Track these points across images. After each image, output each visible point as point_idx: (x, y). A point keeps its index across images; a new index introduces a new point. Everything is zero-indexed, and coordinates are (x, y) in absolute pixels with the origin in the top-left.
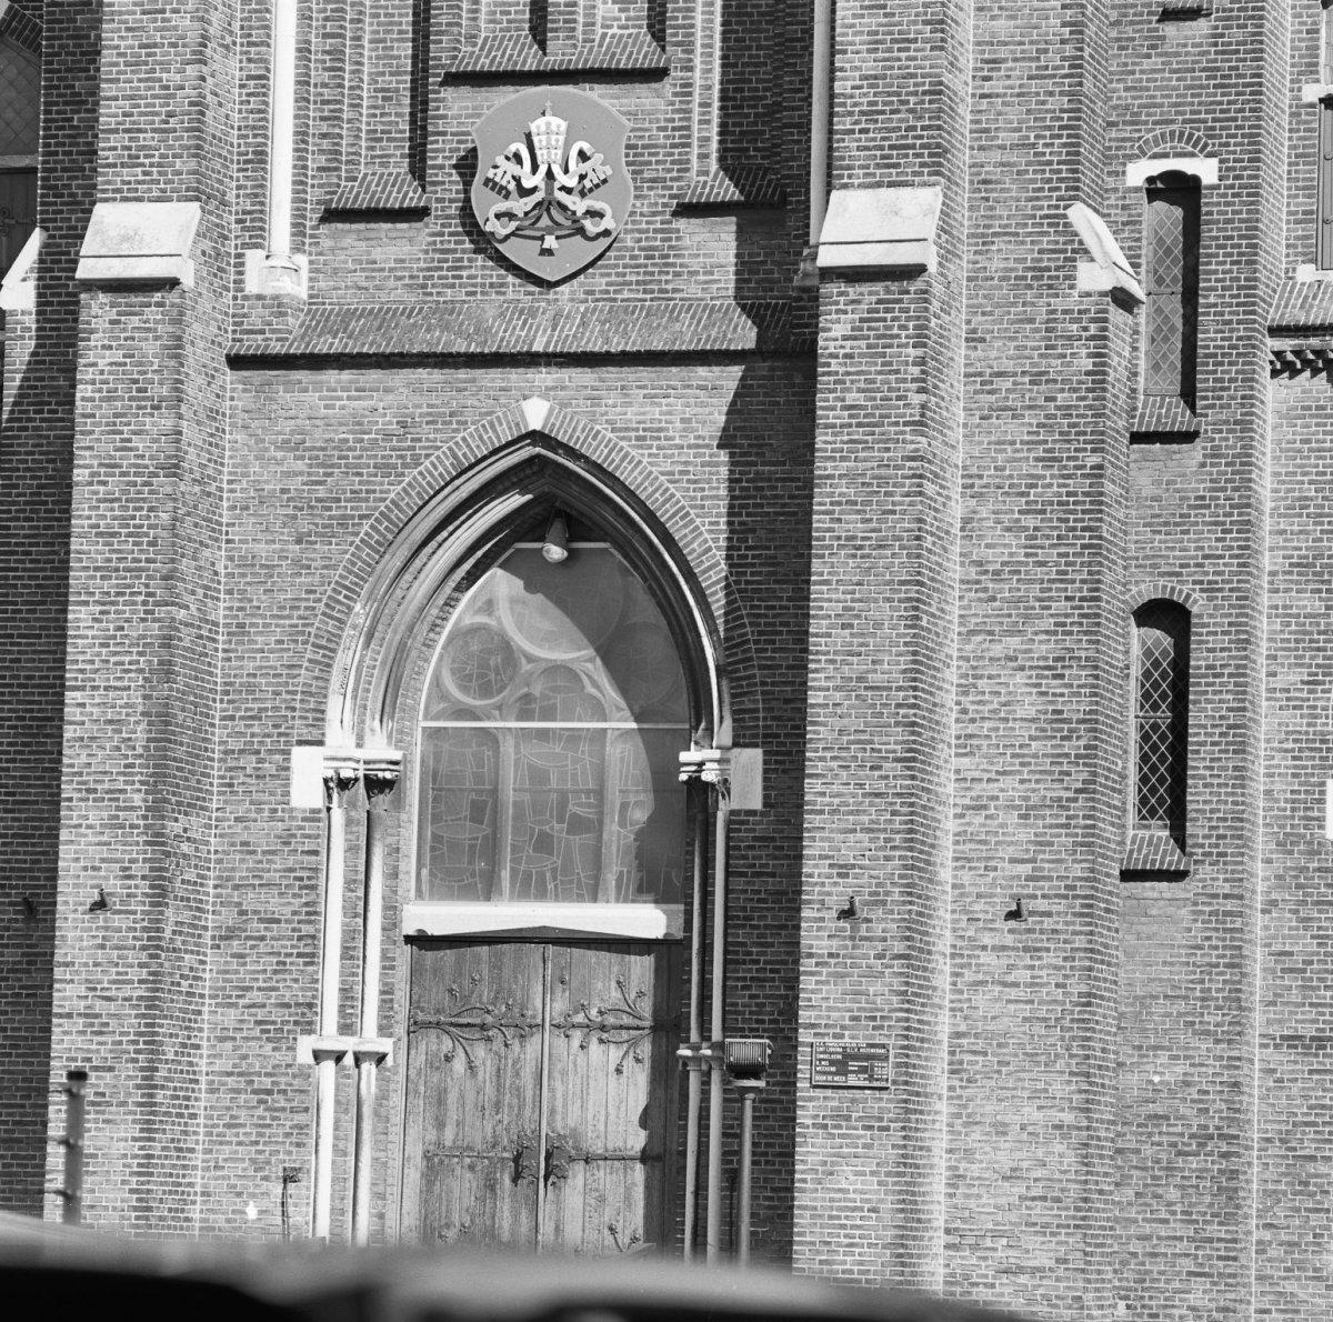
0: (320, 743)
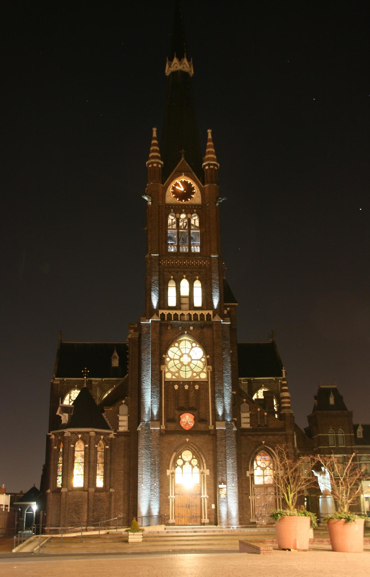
0: (169, 469)
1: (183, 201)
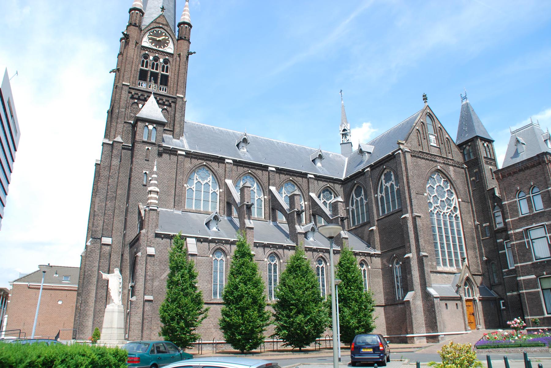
1: (158, 47)
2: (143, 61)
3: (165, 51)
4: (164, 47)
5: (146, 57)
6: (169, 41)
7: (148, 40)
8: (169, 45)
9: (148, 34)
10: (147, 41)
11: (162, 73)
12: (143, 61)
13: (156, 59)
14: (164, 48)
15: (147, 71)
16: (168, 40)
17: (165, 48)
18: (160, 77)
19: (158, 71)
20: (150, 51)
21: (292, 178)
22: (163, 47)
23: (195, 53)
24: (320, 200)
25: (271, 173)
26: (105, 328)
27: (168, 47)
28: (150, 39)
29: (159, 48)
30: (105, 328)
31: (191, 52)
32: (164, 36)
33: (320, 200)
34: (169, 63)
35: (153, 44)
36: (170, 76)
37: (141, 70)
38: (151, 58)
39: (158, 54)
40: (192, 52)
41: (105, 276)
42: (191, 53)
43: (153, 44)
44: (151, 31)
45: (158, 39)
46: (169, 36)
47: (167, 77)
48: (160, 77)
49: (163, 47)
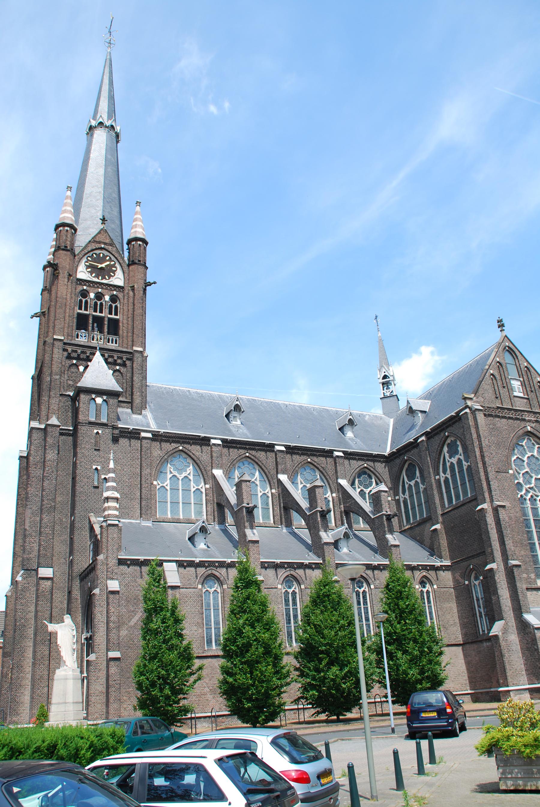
1: (100, 278)
2: (81, 301)
3: (111, 283)
4: (110, 277)
5: (84, 294)
6: (116, 267)
7: (85, 268)
8: (117, 273)
9: (84, 260)
10: (85, 271)
11: (109, 316)
12: (81, 301)
13: (99, 296)
14: (109, 278)
15: (87, 316)
16: (114, 266)
17: (111, 279)
18: (106, 323)
19: (103, 315)
20: (89, 286)
21: (311, 459)
22: (107, 278)
23: (155, 283)
24: (355, 488)
25: (279, 455)
26: (55, 704)
27: (116, 276)
28: (88, 267)
29: (102, 279)
30: (55, 704)
31: (149, 282)
32: (108, 261)
33: (355, 488)
34: (118, 301)
35: (94, 275)
36: (121, 320)
37: (79, 314)
38: (92, 295)
39: (102, 288)
40: (152, 282)
41: (51, 627)
42: (150, 284)
43: (94, 275)
44: (88, 255)
45: (100, 266)
46: (115, 260)
47: (117, 321)
48: (106, 323)
49: (107, 278)
